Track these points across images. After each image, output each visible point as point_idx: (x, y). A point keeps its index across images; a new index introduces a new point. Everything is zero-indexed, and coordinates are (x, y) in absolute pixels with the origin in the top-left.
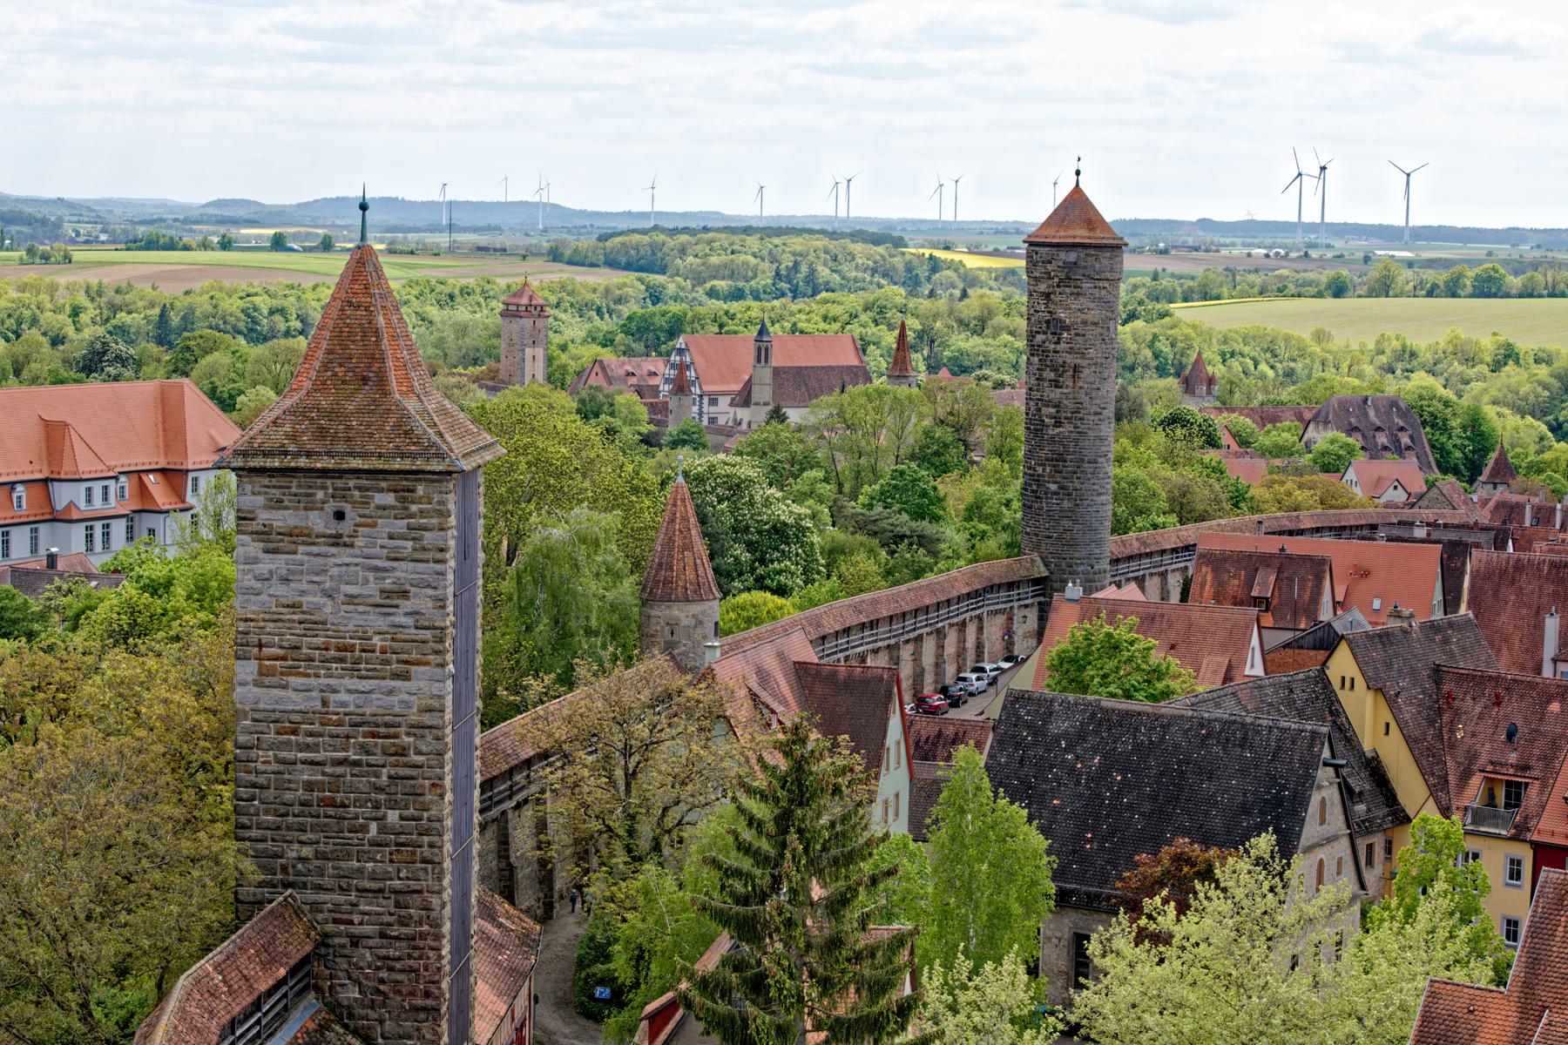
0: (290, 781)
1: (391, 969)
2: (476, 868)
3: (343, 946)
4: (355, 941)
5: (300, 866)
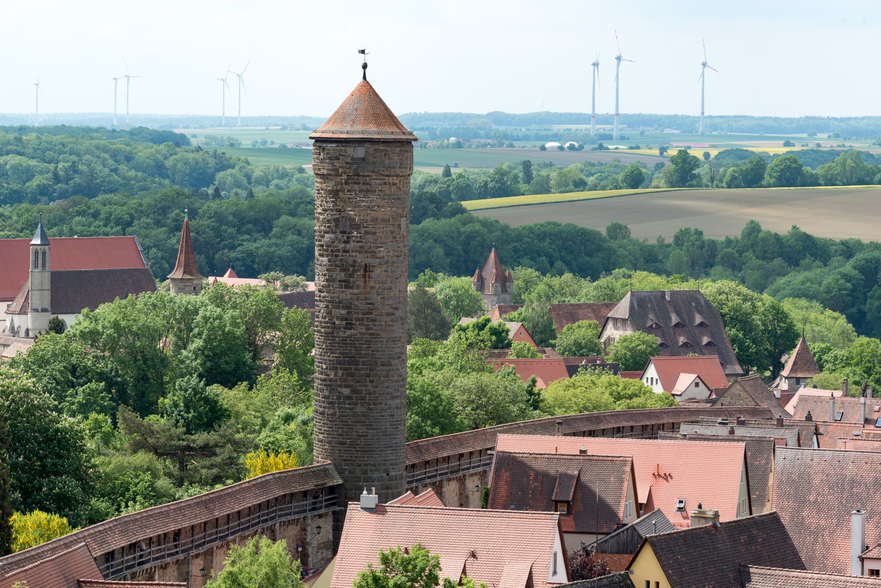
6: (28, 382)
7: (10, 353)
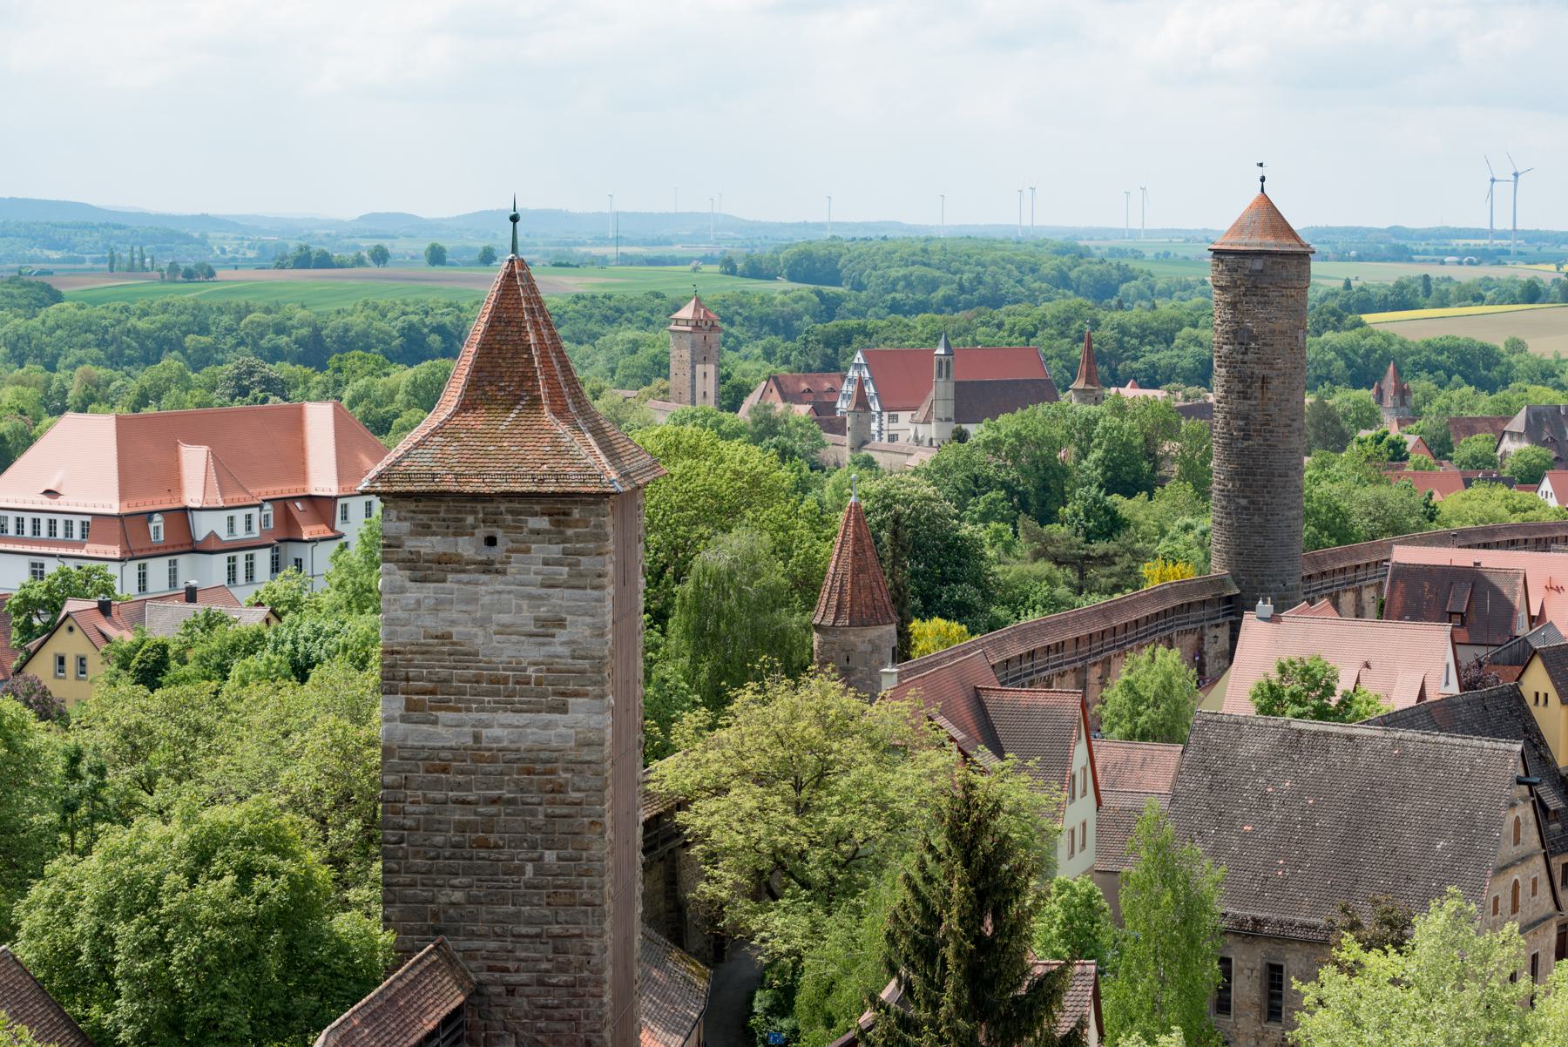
0: (440, 822)
1: (549, 1018)
2: (640, 910)
3: (499, 995)
4: (511, 990)
5: (451, 911)
6: (930, 491)
7: (913, 462)
